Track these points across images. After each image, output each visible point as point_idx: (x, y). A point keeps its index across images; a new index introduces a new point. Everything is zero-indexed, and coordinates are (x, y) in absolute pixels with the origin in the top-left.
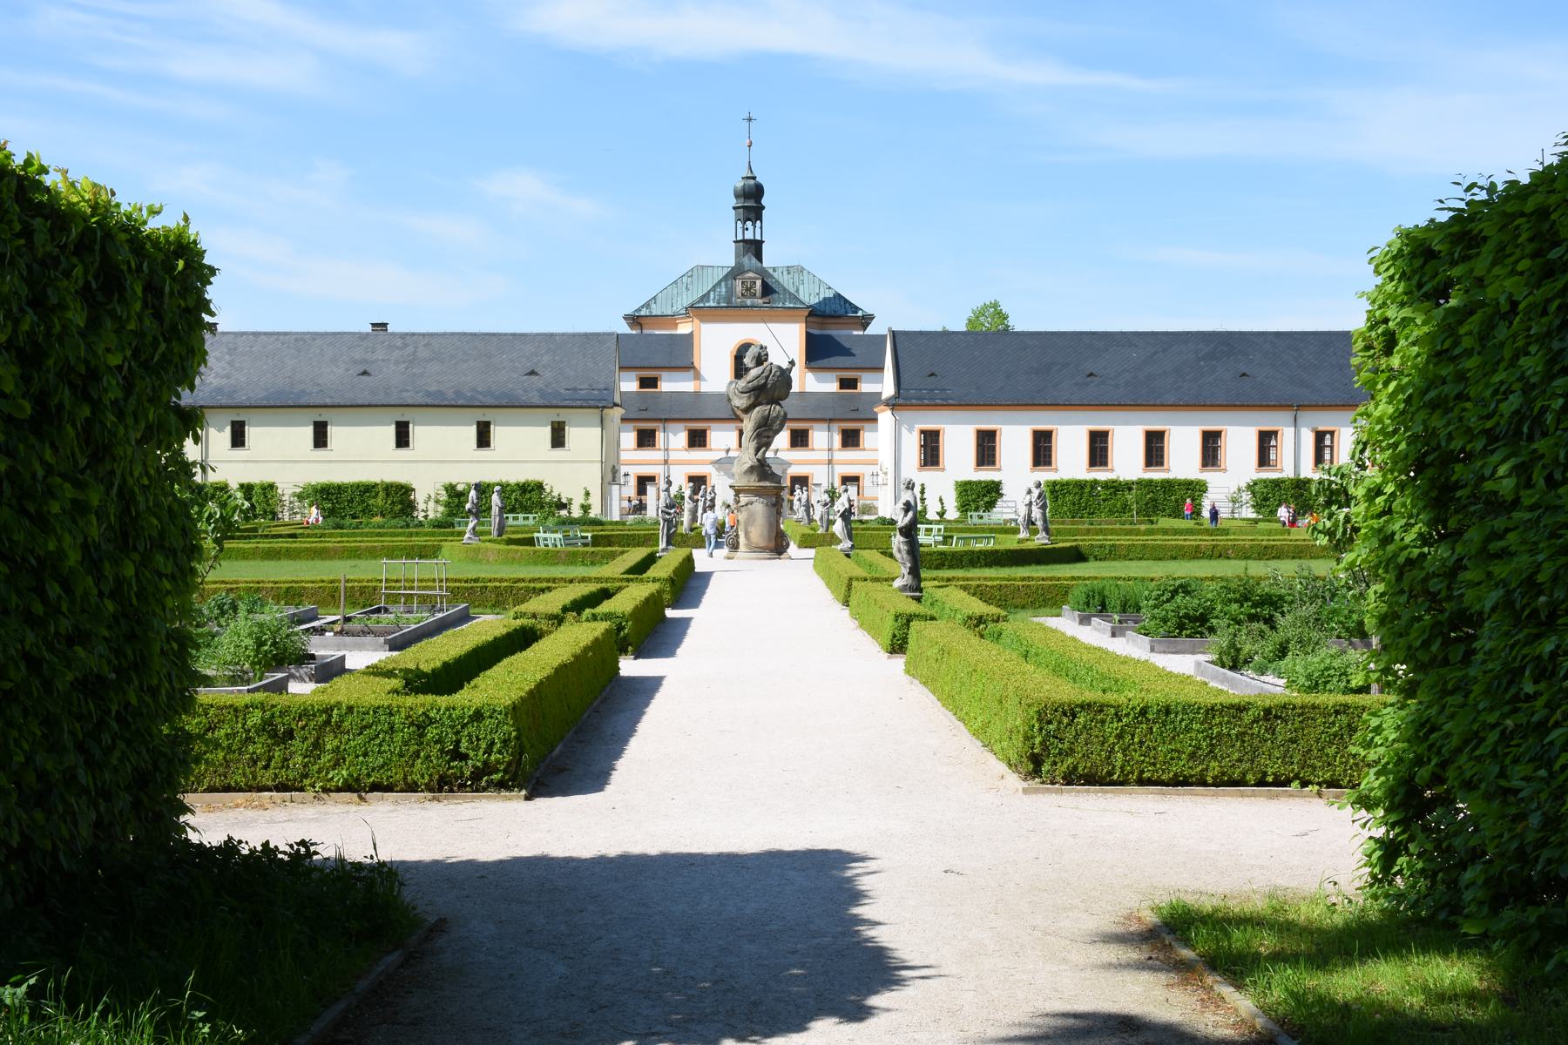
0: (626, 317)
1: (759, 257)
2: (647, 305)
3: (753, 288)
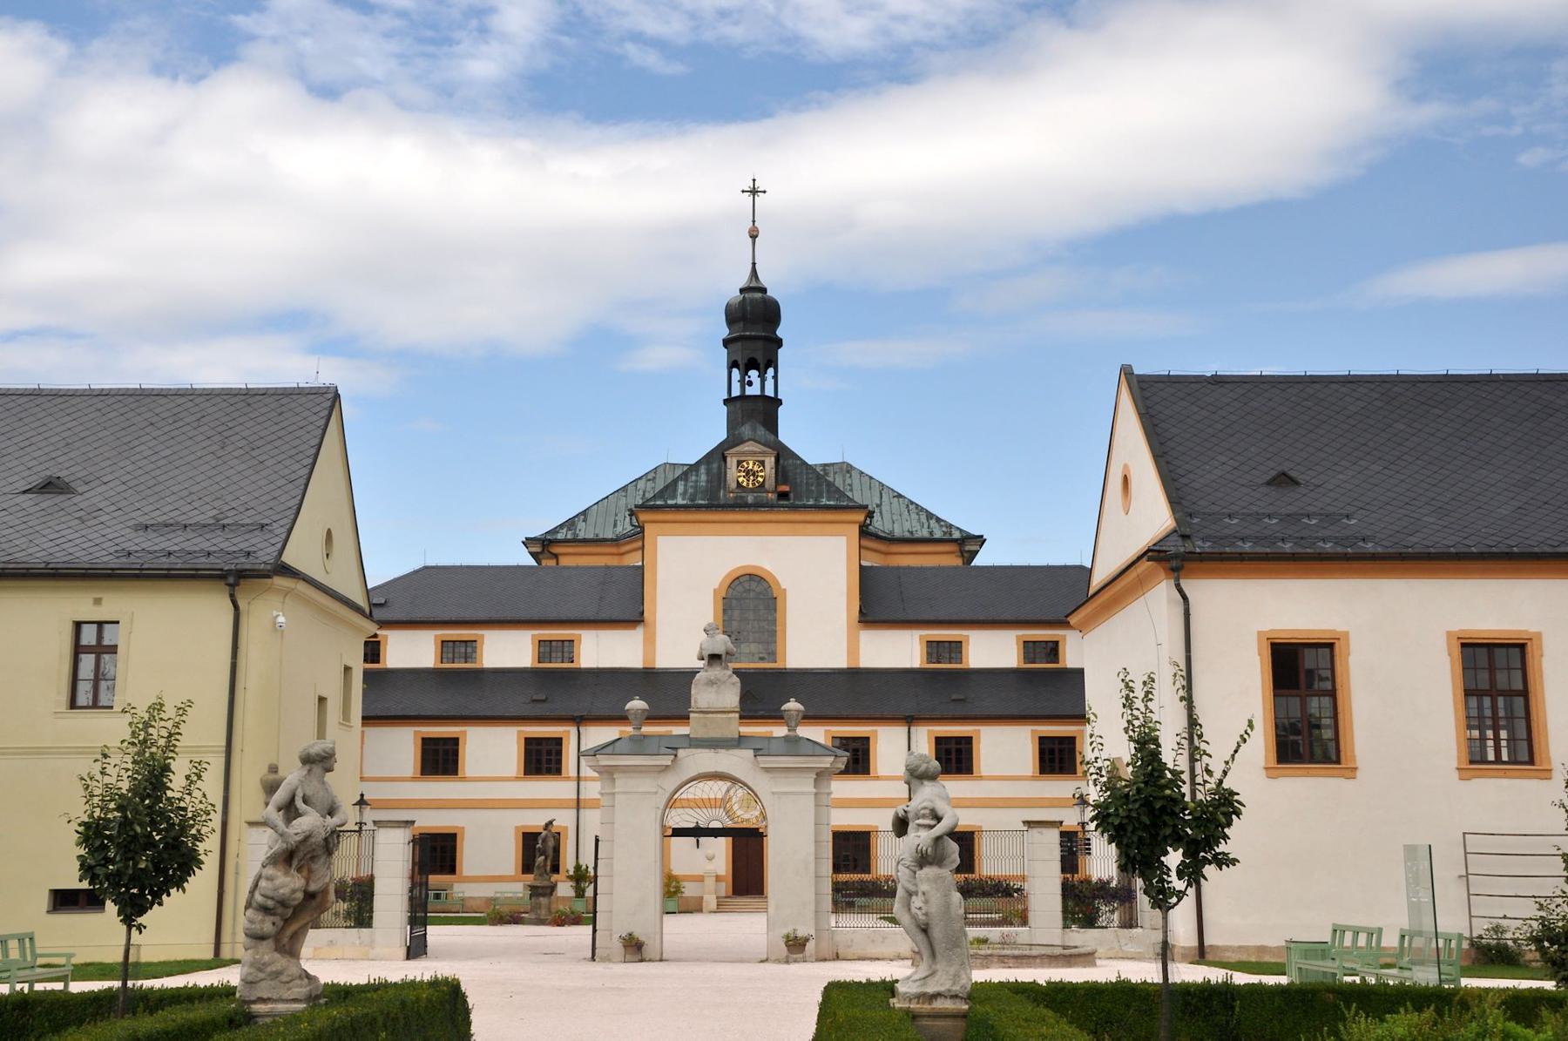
0: (528, 542)
1: (772, 425)
2: (570, 523)
3: (756, 474)
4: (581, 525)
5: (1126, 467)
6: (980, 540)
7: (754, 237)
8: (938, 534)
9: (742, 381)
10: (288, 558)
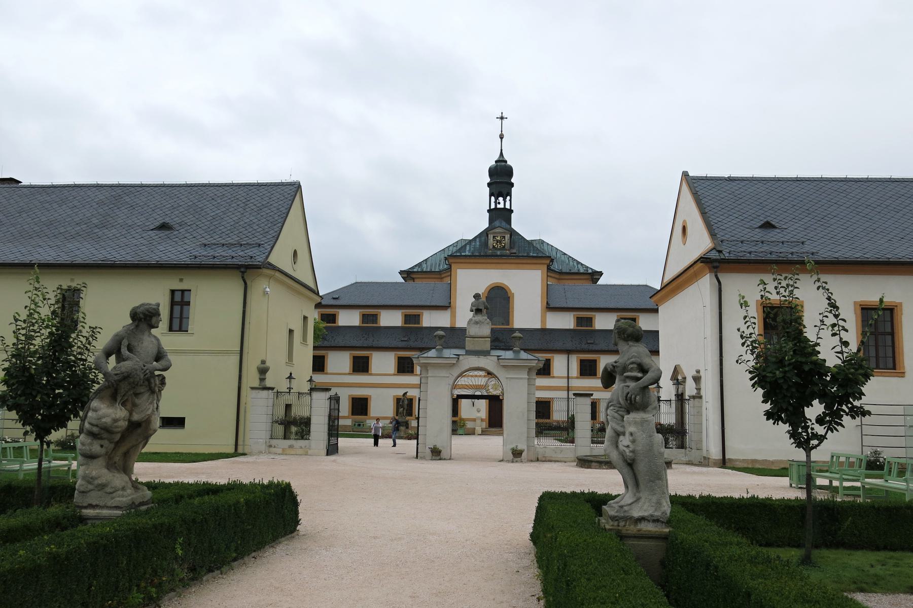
0: (401, 272)
1: (509, 221)
2: (420, 265)
3: (499, 242)
4: (424, 265)
5: (685, 221)
6: (601, 274)
7: (501, 137)
8: (582, 271)
9: (495, 202)
10: (272, 259)
